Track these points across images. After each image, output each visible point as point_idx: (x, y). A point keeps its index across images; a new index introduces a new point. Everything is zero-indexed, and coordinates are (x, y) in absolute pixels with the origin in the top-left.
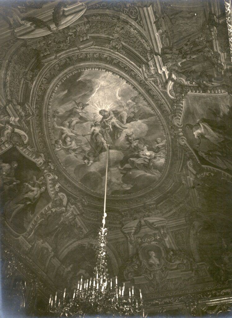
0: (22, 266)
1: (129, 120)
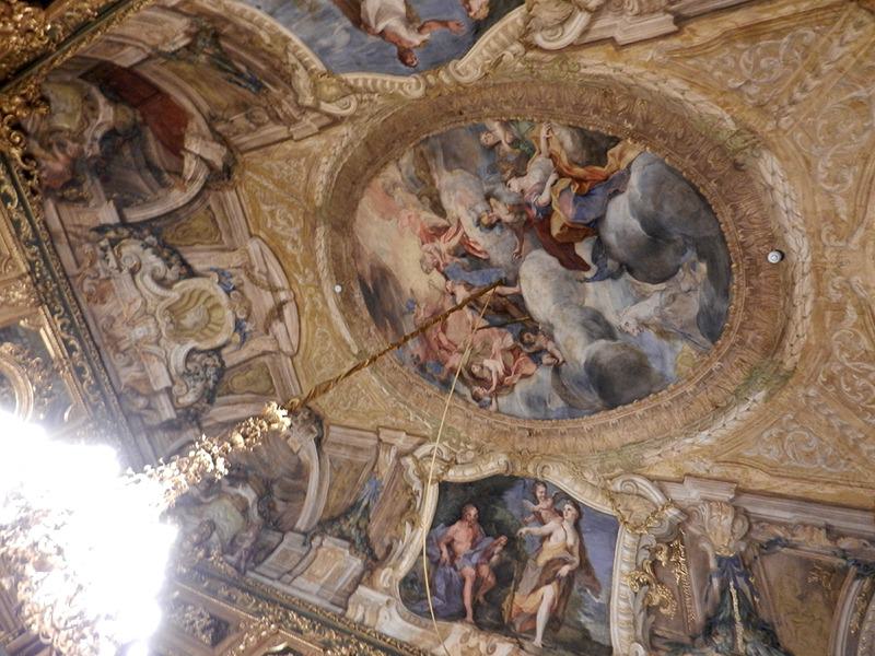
1: (438, 208)
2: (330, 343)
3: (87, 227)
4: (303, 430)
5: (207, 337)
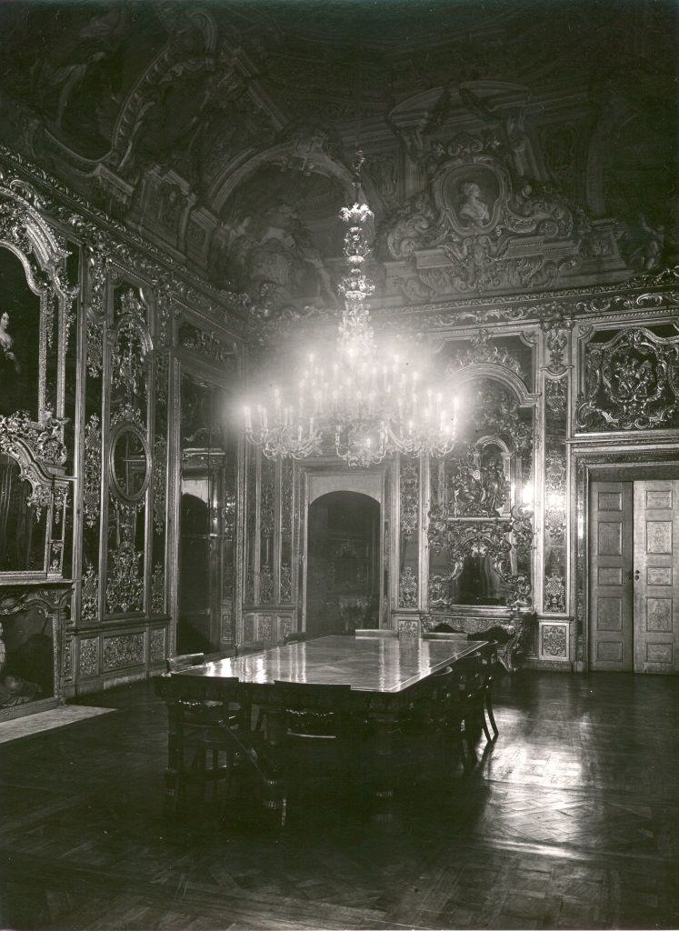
0: (124, 251)
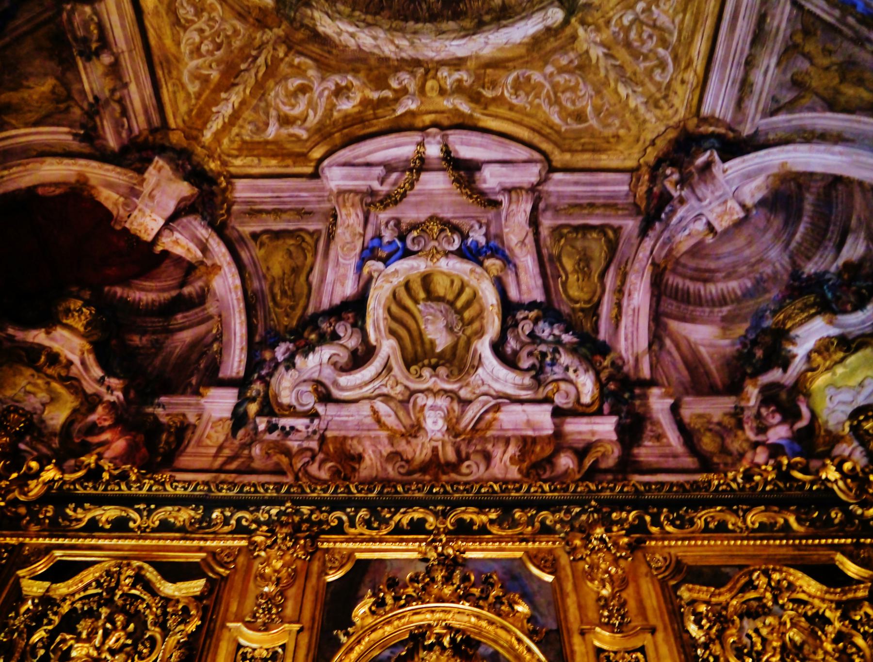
2: (536, 77)
3: (226, 440)
4: (701, 190)
5: (480, 315)
